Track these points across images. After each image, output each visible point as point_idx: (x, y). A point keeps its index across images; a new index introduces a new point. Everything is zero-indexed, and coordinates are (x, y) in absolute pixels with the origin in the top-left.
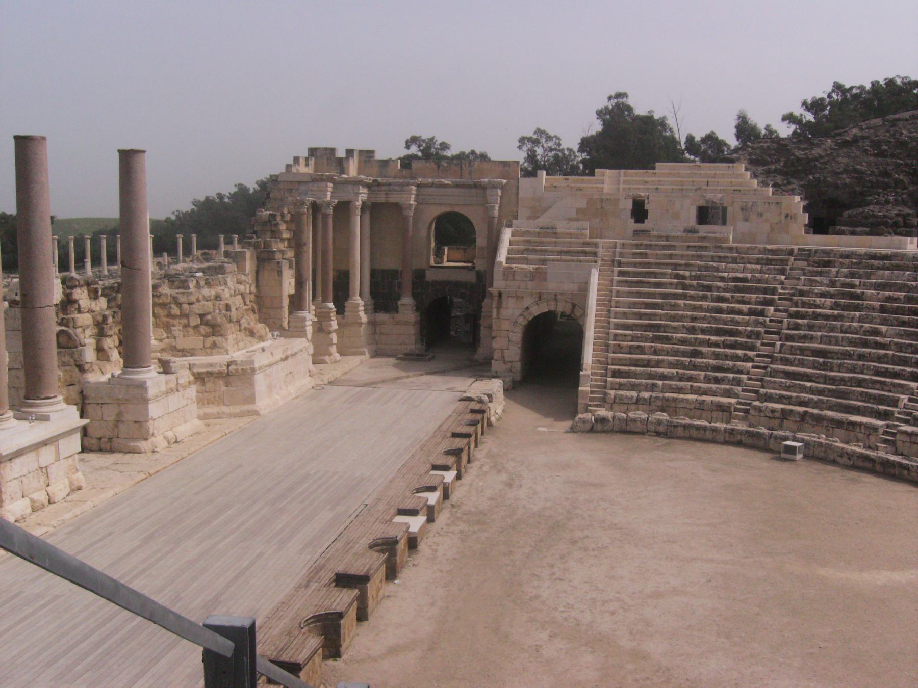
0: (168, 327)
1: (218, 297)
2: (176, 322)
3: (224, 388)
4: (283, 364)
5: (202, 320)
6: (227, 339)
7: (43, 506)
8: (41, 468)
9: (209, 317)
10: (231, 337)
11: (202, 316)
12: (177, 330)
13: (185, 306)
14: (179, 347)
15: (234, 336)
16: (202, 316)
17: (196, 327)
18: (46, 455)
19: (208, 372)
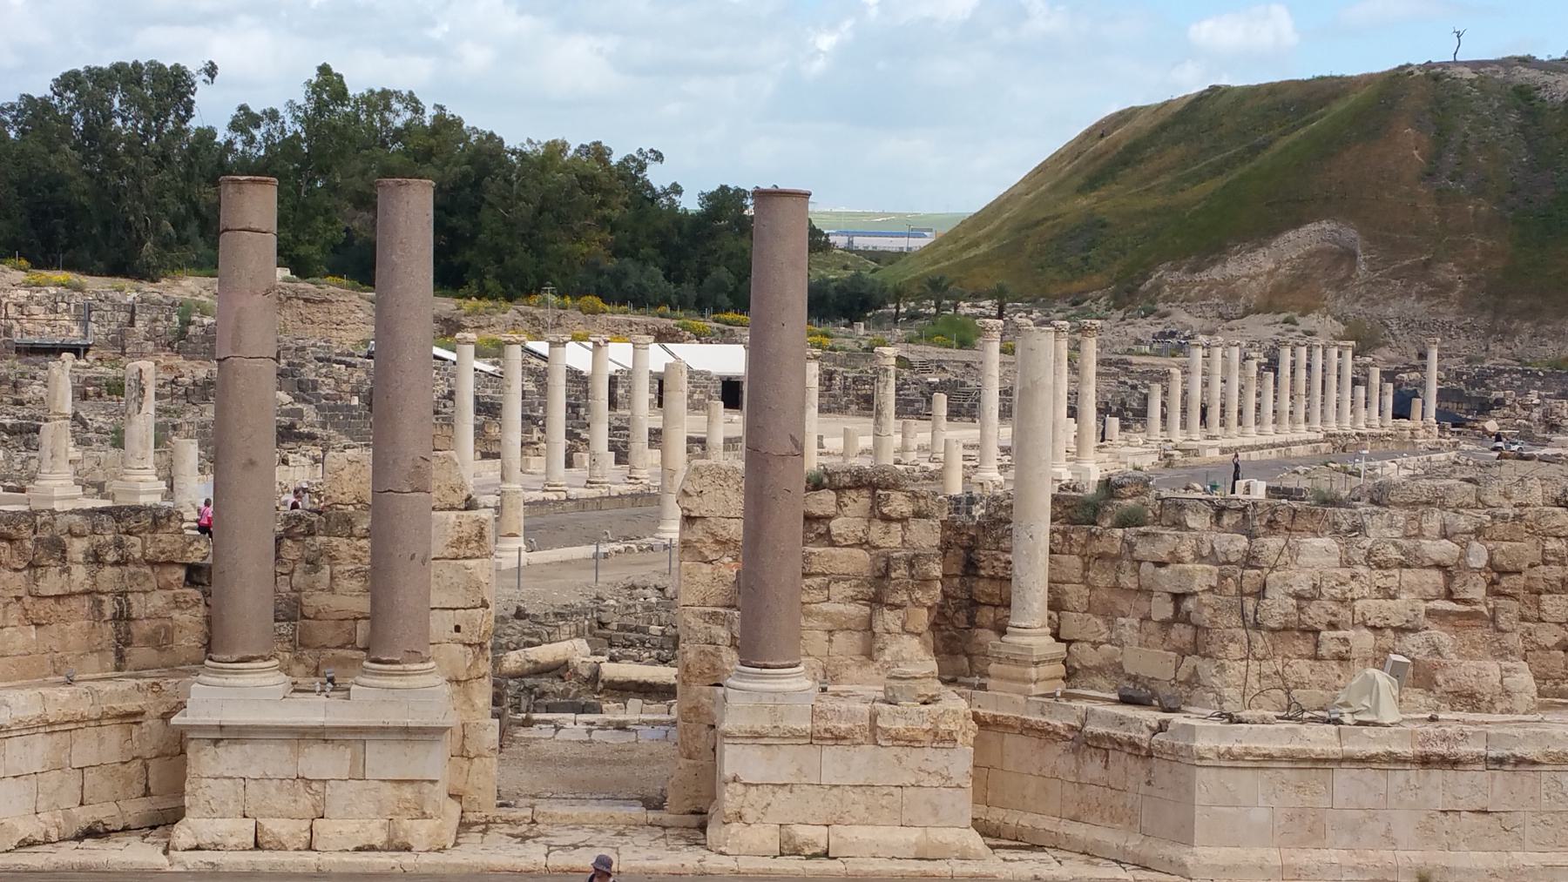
0: (1109, 614)
1: (1250, 560)
2: (1124, 605)
3: (1143, 788)
4: (1415, 775)
5: (1177, 609)
6: (1222, 669)
7: (282, 847)
8: (308, 782)
9: (1189, 604)
10: (1236, 669)
11: (1178, 598)
12: (1128, 625)
13: (1147, 568)
14: (1129, 669)
15: (1267, 668)
16: (1178, 598)
17: (1166, 624)
18: (321, 762)
19: (1111, 739)
